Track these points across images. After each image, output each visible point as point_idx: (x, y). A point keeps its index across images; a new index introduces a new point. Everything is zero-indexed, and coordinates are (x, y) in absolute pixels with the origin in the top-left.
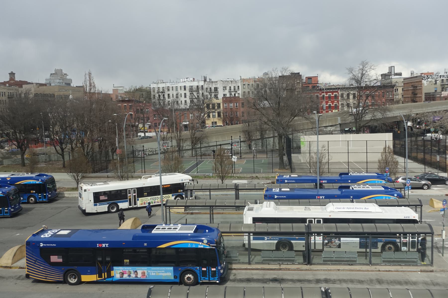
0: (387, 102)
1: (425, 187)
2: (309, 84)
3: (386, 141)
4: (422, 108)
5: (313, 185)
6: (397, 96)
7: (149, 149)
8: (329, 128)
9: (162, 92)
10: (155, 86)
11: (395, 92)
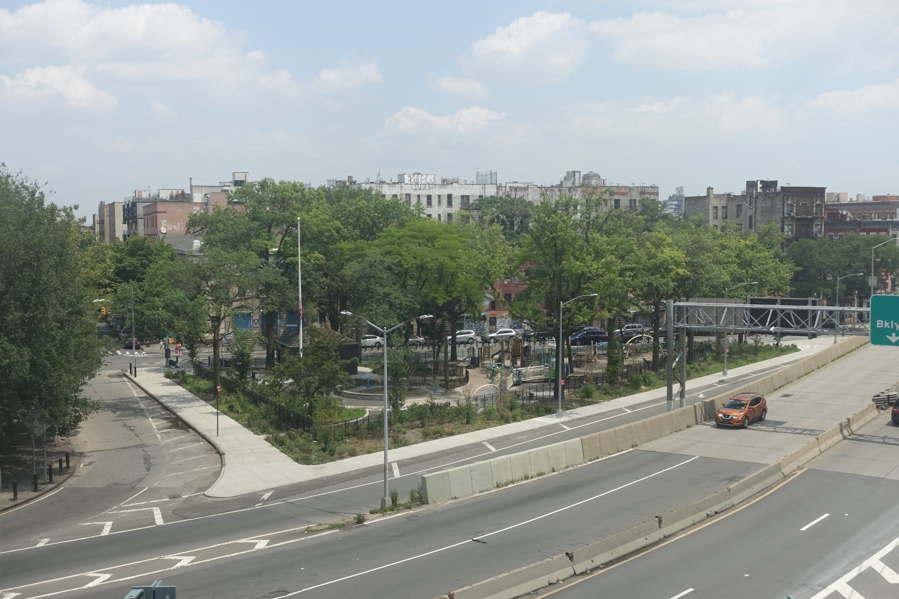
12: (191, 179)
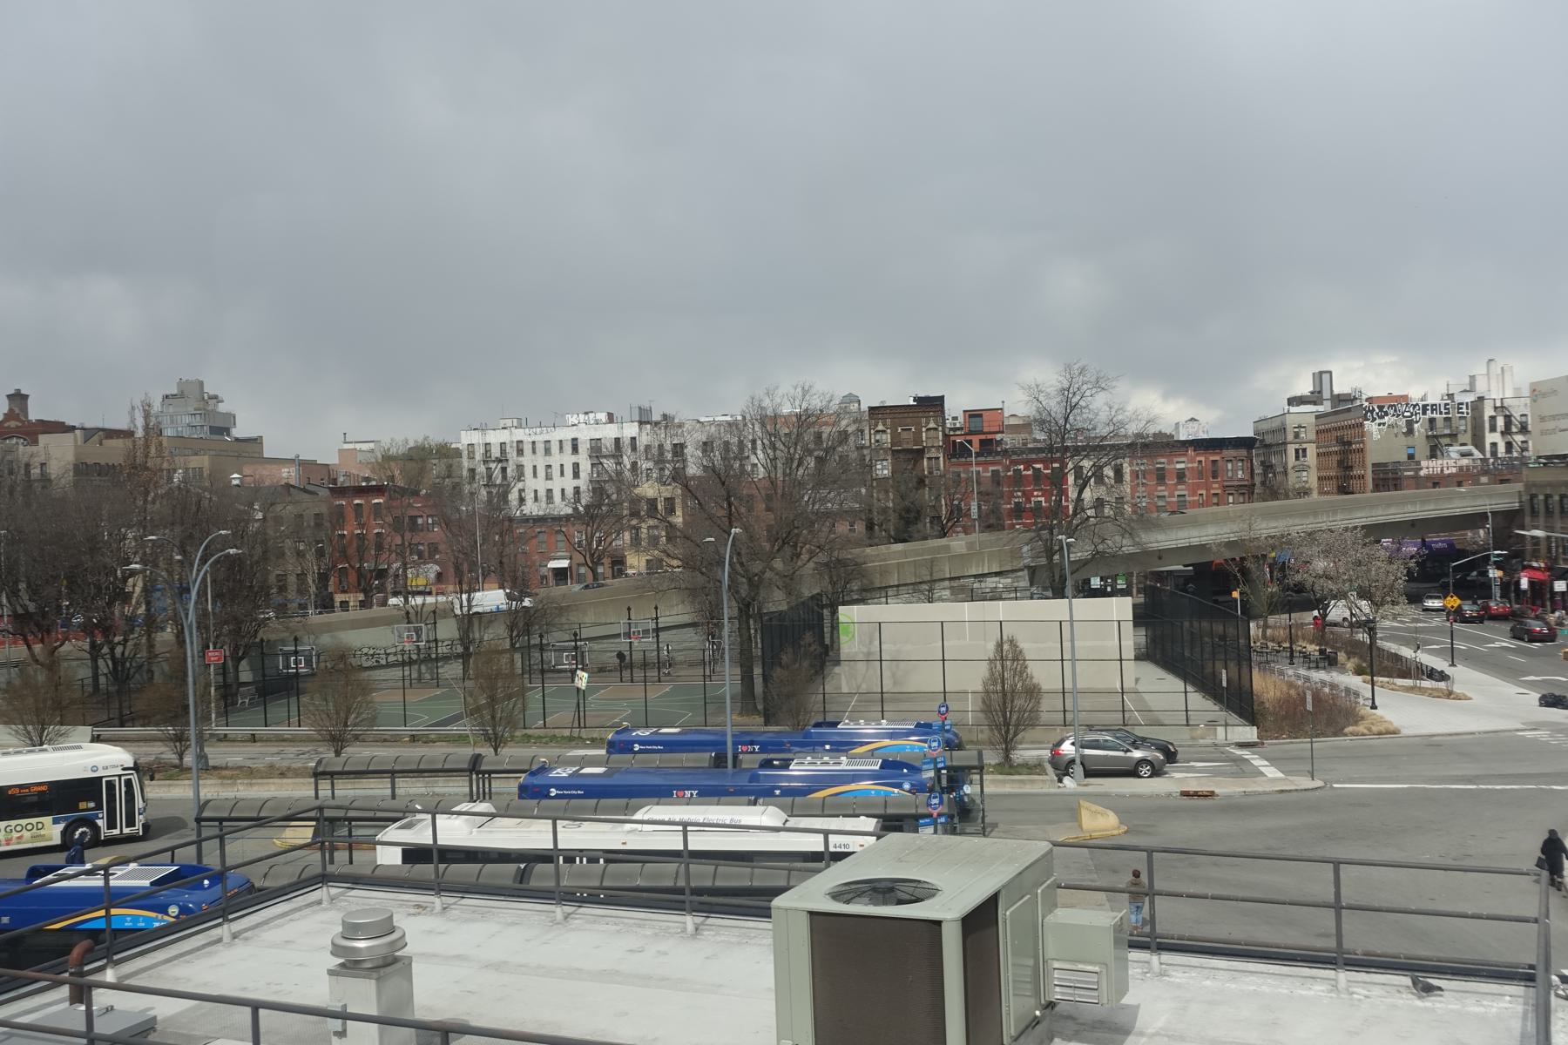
0: (1229, 494)
1: (1145, 770)
2: (971, 433)
3: (1061, 622)
4: (1315, 514)
5: (706, 757)
6: (1305, 474)
7: (365, 651)
8: (991, 582)
9: (499, 461)
10: (475, 438)
11: (1297, 458)
12: (345, 434)
